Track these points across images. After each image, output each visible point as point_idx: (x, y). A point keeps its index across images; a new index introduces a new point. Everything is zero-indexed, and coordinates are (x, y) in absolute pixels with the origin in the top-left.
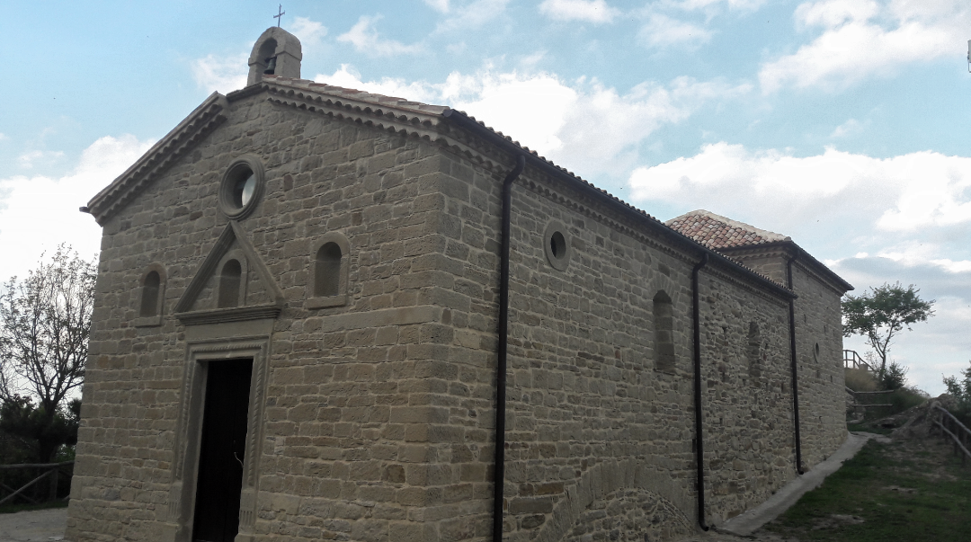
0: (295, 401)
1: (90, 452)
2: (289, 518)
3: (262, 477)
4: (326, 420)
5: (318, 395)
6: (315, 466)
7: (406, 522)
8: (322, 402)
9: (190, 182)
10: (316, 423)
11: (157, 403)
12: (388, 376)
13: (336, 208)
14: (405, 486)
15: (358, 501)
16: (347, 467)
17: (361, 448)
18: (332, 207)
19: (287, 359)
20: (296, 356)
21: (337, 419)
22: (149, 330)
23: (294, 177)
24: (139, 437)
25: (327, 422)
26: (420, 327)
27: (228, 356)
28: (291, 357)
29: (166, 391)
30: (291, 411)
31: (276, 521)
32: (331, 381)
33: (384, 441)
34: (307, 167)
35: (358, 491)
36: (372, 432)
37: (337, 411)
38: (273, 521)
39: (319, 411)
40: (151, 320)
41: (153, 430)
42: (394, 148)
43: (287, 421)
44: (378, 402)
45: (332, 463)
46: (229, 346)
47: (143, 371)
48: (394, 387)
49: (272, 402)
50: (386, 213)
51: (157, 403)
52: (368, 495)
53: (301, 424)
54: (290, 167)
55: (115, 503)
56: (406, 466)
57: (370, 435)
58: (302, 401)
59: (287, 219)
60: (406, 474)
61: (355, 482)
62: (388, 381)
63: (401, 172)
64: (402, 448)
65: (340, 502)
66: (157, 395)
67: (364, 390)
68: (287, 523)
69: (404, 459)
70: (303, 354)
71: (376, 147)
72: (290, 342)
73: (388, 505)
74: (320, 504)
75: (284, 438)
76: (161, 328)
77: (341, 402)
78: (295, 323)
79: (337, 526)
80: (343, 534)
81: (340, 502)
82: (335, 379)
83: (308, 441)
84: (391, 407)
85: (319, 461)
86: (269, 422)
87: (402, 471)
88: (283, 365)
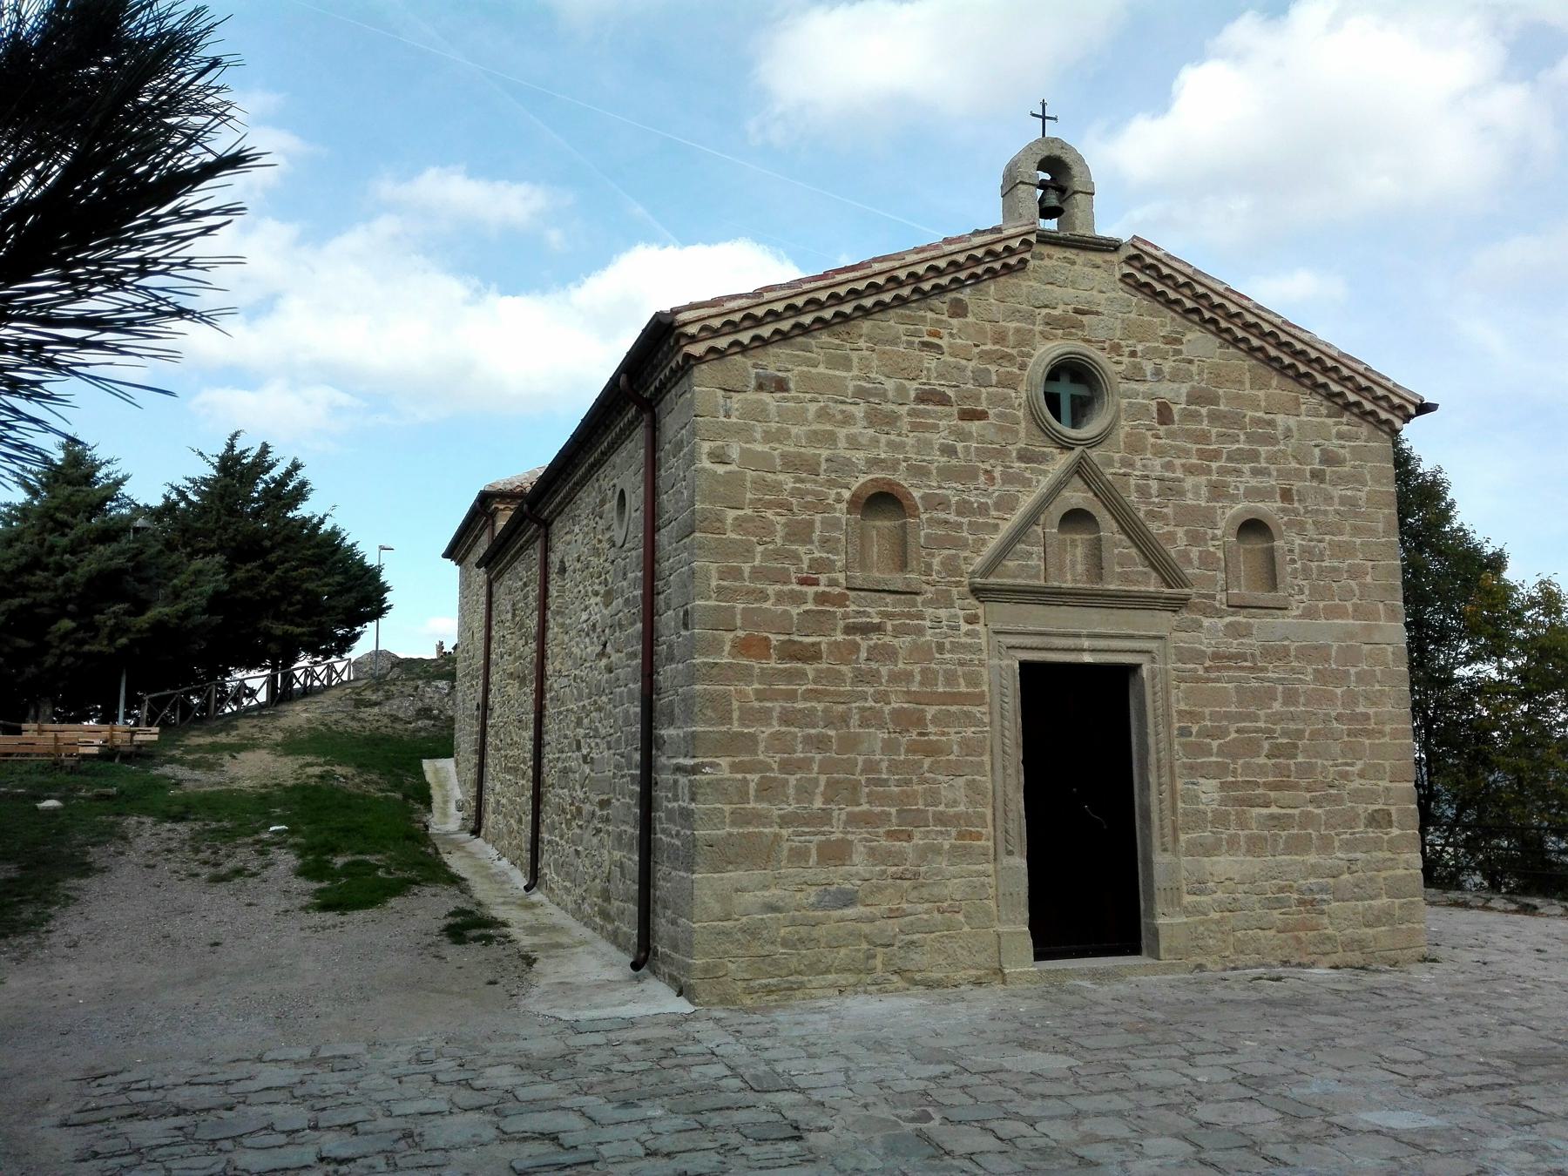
0: (1225, 732)
1: (749, 823)
2: (1241, 888)
3: (1183, 837)
4: (1278, 757)
5: (1262, 724)
6: (1272, 817)
7: (1400, 872)
8: (1270, 734)
9: (946, 349)
10: (1262, 760)
11: (931, 729)
12: (1356, 704)
13: (1256, 472)
14: (1395, 832)
15: (1339, 855)
16: (1319, 815)
17: (1333, 791)
18: (1246, 467)
19: (1201, 672)
20: (1218, 669)
21: (1294, 756)
22: (889, 598)
23: (1176, 409)
24: (896, 789)
25: (1281, 760)
26: (1390, 649)
27: (1088, 658)
28: (1207, 670)
29: (953, 708)
30: (1220, 745)
31: (1219, 895)
32: (1277, 706)
33: (1362, 781)
34: (1196, 398)
35: (1337, 844)
36: (1347, 772)
37: (1295, 746)
38: (1215, 896)
39: (1266, 745)
40: (897, 580)
41: (927, 775)
42: (1329, 416)
43: (1213, 759)
44: (1348, 735)
45: (1296, 812)
46: (1086, 643)
47: (884, 671)
48: (1366, 717)
49: (1185, 732)
50: (1329, 499)
51: (931, 729)
52: (1349, 846)
53: (1240, 762)
54: (1166, 390)
55: (849, 912)
56: (1393, 809)
57: (1345, 776)
58: (1237, 731)
59: (1168, 466)
60: (1394, 818)
61: (1333, 833)
62: (1358, 710)
63: (1343, 451)
64: (1387, 789)
65: (1312, 858)
66: (929, 717)
67: (1327, 719)
68: (1239, 896)
69: (1392, 801)
70: (1230, 668)
71: (1304, 407)
72: (1203, 648)
73: (1380, 855)
74: (1289, 865)
75: (1216, 782)
76: (919, 599)
77: (1299, 734)
78: (1206, 622)
79: (1314, 887)
80: (1325, 897)
81: (1312, 858)
82: (1285, 704)
83: (1257, 784)
84: (1367, 742)
85: (1274, 810)
86: (1185, 760)
87: (1389, 815)
88: (1198, 680)
